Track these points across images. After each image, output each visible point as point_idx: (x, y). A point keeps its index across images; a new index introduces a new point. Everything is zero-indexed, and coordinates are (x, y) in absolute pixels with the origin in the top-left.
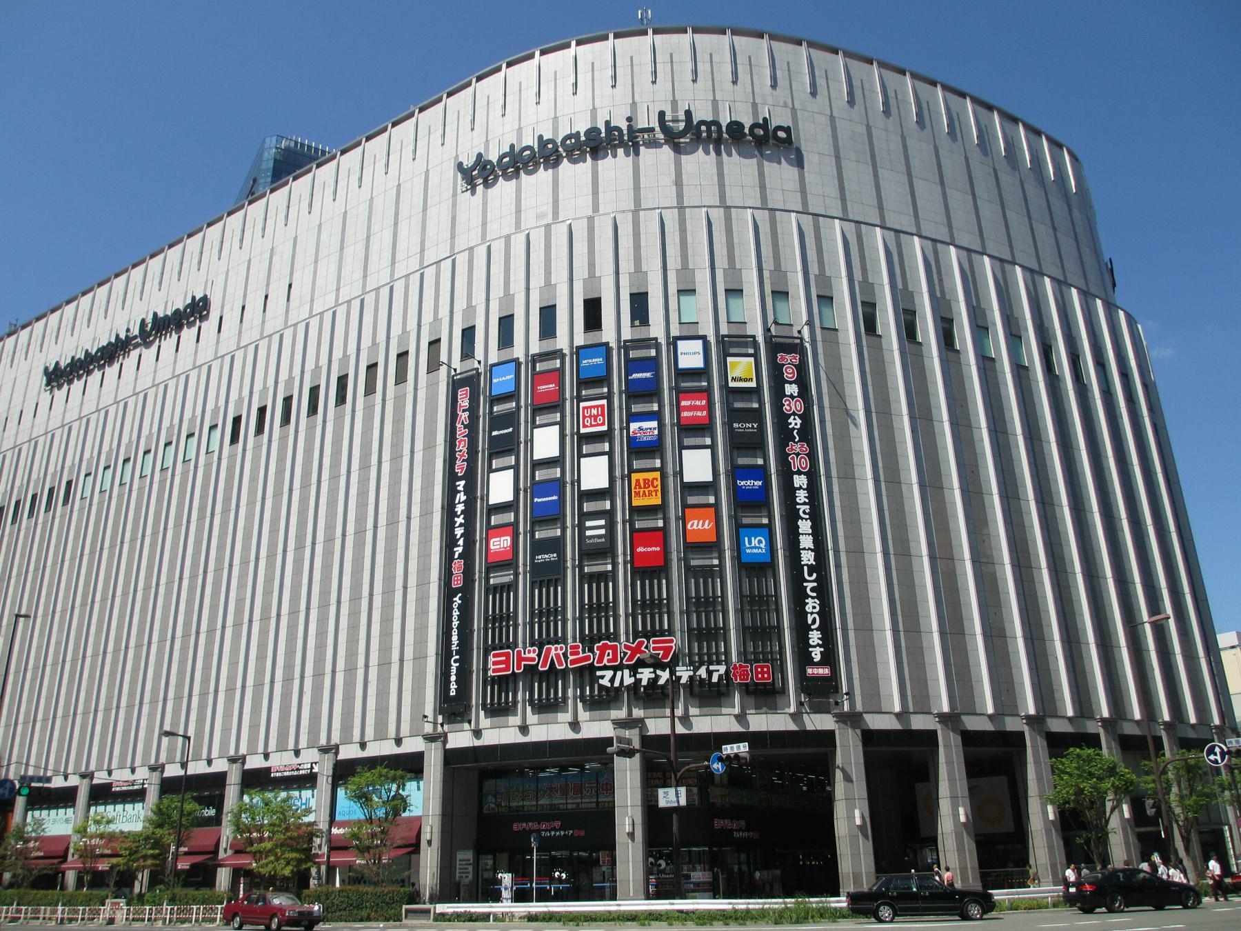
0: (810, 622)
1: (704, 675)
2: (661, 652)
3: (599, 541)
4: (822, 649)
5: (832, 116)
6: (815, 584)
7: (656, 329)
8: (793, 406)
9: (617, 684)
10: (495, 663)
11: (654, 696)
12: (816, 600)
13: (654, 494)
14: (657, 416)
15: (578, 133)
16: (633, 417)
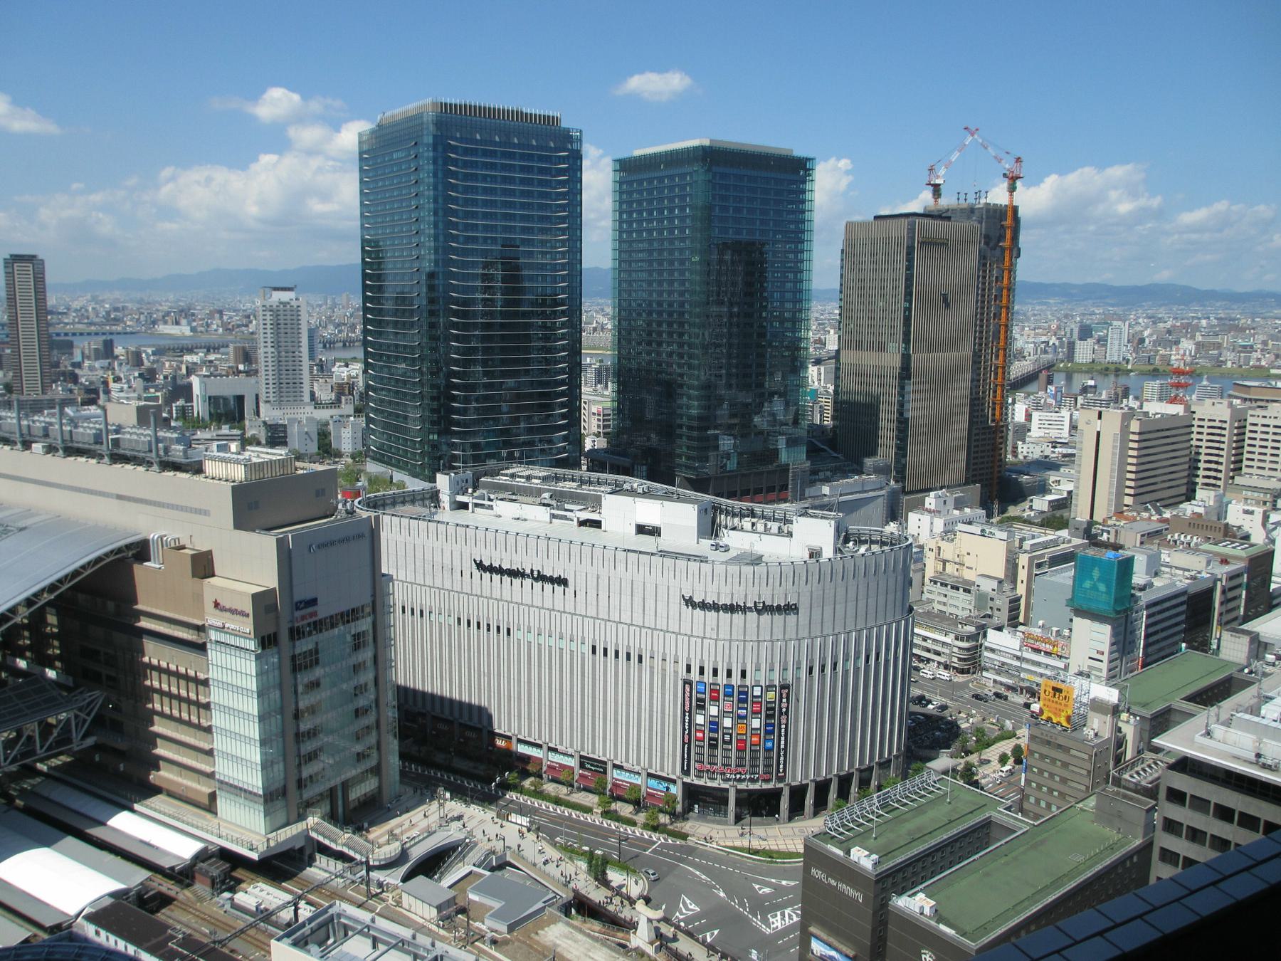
7: (748, 682)
8: (784, 705)
11: (740, 780)
14: (746, 709)
16: (739, 708)
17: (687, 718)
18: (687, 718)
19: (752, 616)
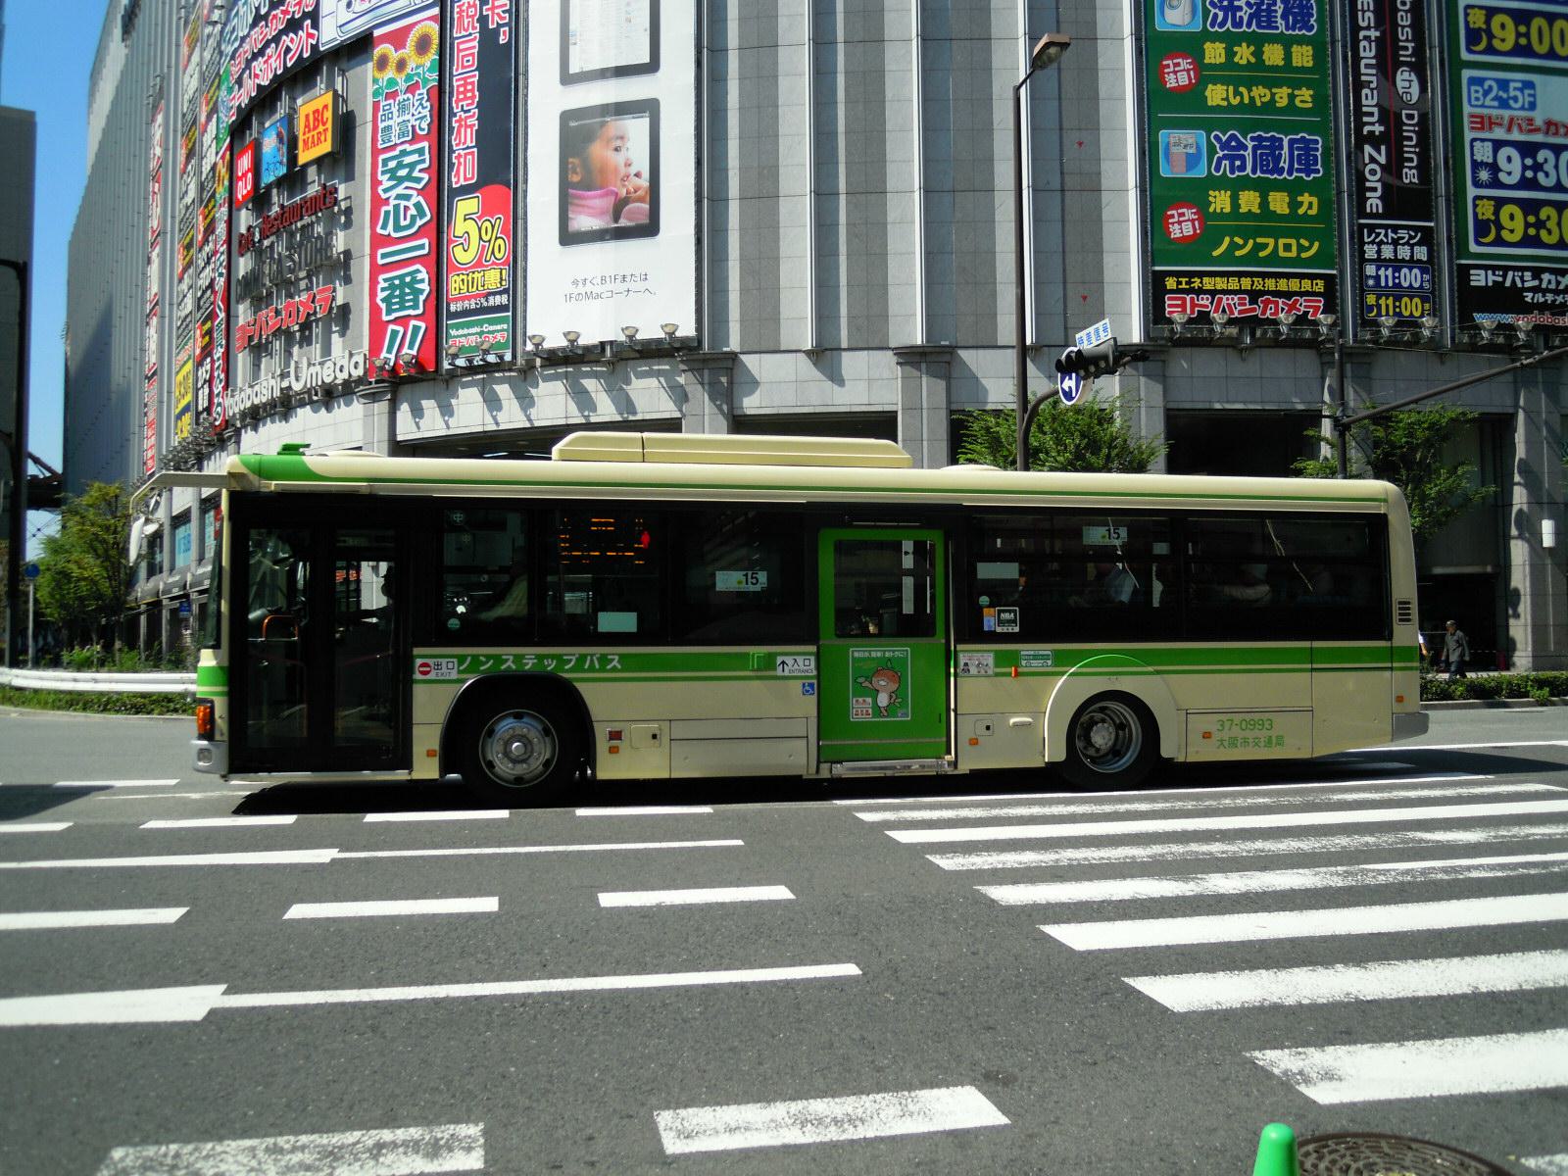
10: (1170, 306)
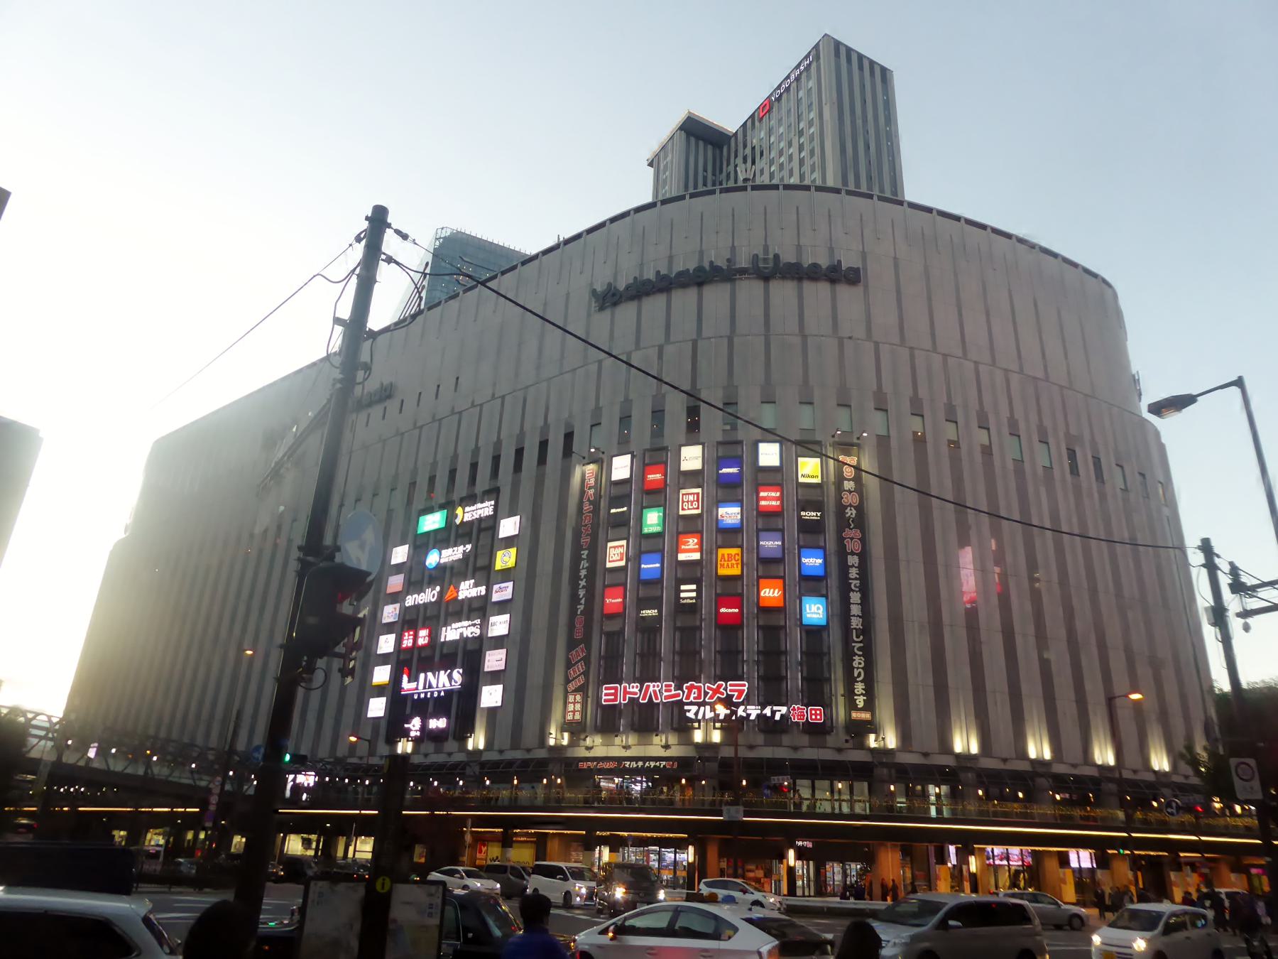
0: (856, 675)
1: (769, 714)
2: (736, 694)
3: (691, 601)
4: (865, 698)
5: (895, 258)
6: (862, 645)
9: (700, 717)
10: (606, 695)
12: (862, 658)
13: (735, 566)
15: (688, 270)
17: (584, 564)
18: (584, 564)
19: (750, 290)
